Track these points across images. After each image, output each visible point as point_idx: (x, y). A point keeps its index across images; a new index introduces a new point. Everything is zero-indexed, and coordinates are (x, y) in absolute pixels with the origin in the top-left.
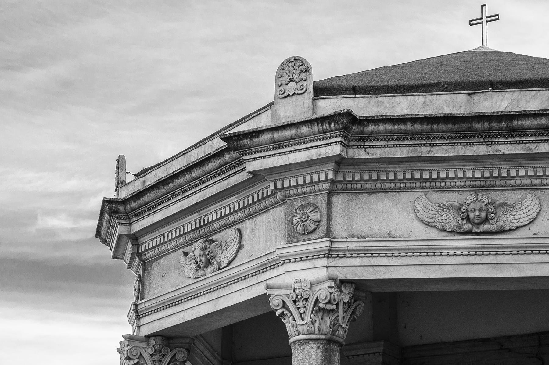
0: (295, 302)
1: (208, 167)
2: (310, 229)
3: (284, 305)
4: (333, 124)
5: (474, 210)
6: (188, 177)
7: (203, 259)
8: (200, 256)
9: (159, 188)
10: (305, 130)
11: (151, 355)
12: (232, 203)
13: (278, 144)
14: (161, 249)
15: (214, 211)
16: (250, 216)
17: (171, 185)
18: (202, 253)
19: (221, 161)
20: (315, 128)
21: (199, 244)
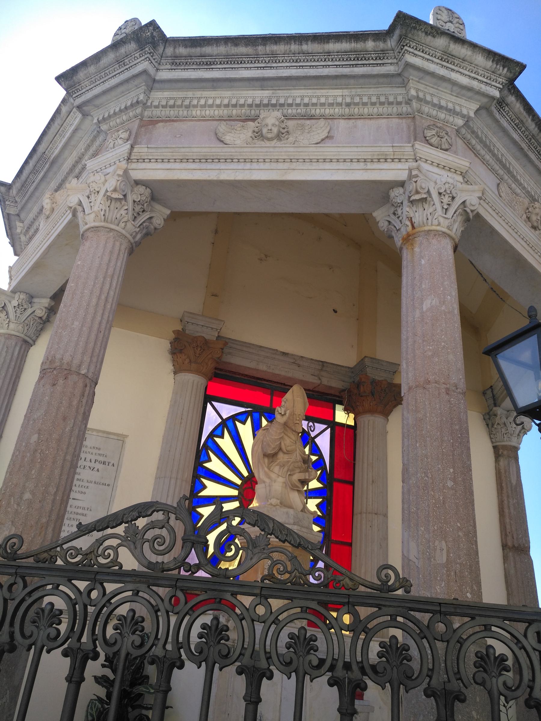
0: (440, 194)
1: (332, 46)
2: (443, 147)
3: (428, 192)
4: (506, 70)
5: (537, 214)
6: (294, 47)
7: (275, 130)
8: (273, 125)
9: (236, 45)
10: (480, 59)
11: (134, 201)
12: (337, 94)
13: (447, 57)
14: (183, 112)
15: (298, 94)
16: (350, 117)
17: (260, 48)
18: (277, 123)
19: (359, 46)
20: (489, 64)
21: (277, 114)
